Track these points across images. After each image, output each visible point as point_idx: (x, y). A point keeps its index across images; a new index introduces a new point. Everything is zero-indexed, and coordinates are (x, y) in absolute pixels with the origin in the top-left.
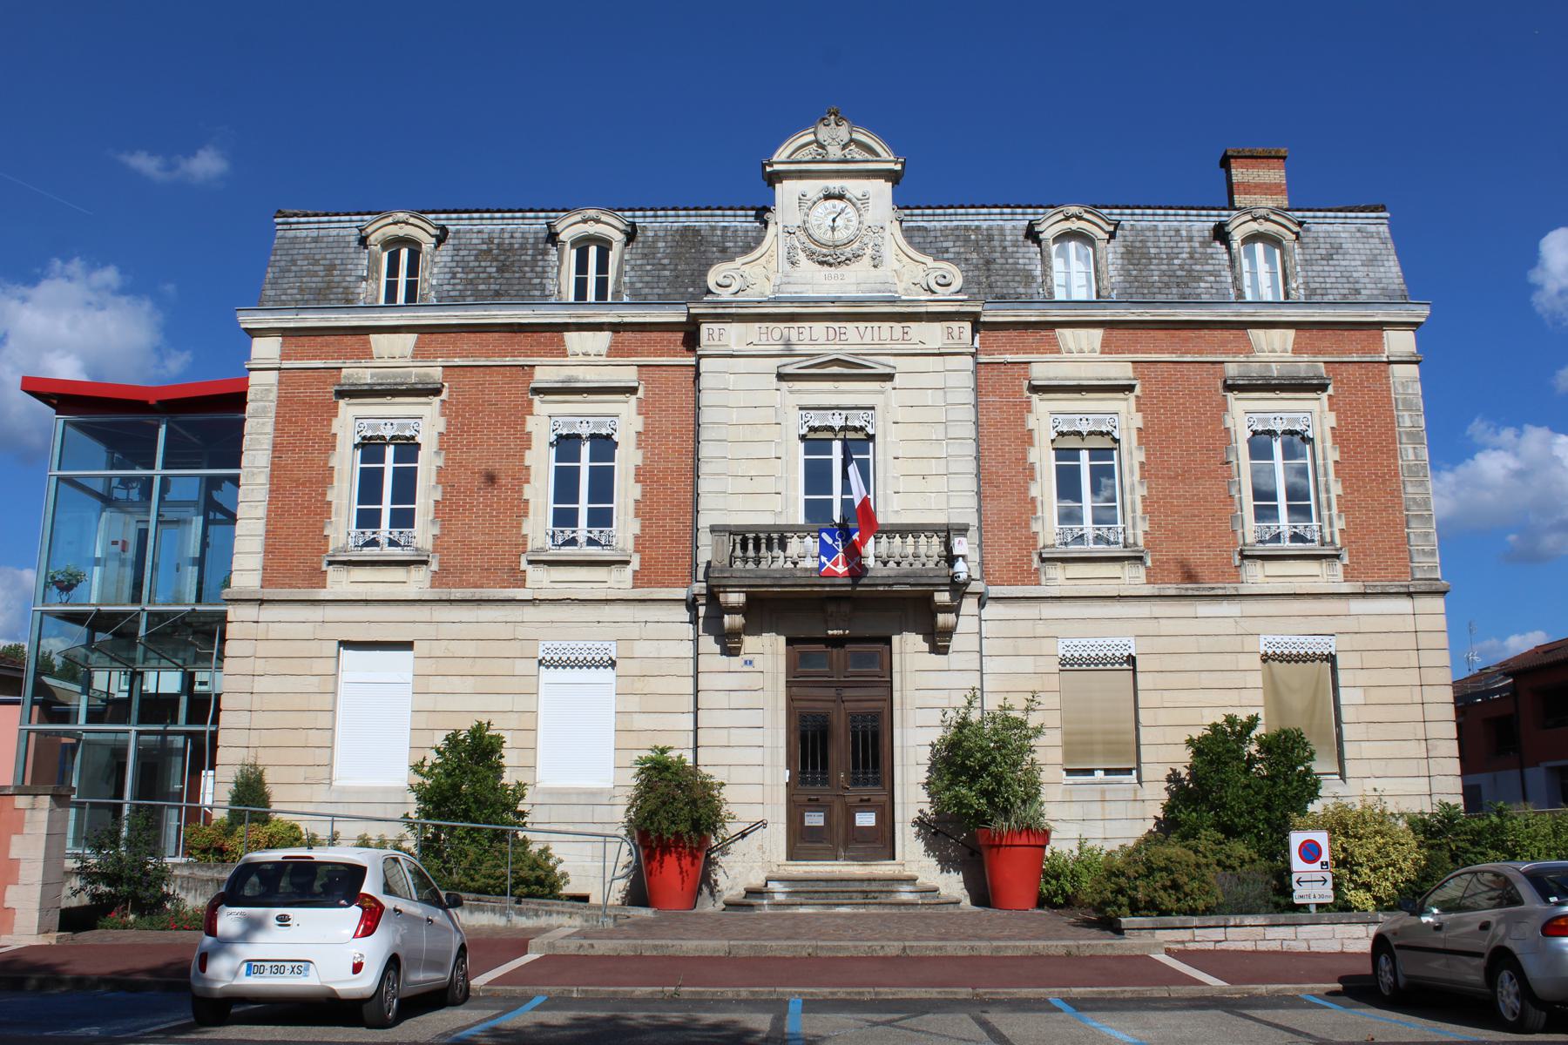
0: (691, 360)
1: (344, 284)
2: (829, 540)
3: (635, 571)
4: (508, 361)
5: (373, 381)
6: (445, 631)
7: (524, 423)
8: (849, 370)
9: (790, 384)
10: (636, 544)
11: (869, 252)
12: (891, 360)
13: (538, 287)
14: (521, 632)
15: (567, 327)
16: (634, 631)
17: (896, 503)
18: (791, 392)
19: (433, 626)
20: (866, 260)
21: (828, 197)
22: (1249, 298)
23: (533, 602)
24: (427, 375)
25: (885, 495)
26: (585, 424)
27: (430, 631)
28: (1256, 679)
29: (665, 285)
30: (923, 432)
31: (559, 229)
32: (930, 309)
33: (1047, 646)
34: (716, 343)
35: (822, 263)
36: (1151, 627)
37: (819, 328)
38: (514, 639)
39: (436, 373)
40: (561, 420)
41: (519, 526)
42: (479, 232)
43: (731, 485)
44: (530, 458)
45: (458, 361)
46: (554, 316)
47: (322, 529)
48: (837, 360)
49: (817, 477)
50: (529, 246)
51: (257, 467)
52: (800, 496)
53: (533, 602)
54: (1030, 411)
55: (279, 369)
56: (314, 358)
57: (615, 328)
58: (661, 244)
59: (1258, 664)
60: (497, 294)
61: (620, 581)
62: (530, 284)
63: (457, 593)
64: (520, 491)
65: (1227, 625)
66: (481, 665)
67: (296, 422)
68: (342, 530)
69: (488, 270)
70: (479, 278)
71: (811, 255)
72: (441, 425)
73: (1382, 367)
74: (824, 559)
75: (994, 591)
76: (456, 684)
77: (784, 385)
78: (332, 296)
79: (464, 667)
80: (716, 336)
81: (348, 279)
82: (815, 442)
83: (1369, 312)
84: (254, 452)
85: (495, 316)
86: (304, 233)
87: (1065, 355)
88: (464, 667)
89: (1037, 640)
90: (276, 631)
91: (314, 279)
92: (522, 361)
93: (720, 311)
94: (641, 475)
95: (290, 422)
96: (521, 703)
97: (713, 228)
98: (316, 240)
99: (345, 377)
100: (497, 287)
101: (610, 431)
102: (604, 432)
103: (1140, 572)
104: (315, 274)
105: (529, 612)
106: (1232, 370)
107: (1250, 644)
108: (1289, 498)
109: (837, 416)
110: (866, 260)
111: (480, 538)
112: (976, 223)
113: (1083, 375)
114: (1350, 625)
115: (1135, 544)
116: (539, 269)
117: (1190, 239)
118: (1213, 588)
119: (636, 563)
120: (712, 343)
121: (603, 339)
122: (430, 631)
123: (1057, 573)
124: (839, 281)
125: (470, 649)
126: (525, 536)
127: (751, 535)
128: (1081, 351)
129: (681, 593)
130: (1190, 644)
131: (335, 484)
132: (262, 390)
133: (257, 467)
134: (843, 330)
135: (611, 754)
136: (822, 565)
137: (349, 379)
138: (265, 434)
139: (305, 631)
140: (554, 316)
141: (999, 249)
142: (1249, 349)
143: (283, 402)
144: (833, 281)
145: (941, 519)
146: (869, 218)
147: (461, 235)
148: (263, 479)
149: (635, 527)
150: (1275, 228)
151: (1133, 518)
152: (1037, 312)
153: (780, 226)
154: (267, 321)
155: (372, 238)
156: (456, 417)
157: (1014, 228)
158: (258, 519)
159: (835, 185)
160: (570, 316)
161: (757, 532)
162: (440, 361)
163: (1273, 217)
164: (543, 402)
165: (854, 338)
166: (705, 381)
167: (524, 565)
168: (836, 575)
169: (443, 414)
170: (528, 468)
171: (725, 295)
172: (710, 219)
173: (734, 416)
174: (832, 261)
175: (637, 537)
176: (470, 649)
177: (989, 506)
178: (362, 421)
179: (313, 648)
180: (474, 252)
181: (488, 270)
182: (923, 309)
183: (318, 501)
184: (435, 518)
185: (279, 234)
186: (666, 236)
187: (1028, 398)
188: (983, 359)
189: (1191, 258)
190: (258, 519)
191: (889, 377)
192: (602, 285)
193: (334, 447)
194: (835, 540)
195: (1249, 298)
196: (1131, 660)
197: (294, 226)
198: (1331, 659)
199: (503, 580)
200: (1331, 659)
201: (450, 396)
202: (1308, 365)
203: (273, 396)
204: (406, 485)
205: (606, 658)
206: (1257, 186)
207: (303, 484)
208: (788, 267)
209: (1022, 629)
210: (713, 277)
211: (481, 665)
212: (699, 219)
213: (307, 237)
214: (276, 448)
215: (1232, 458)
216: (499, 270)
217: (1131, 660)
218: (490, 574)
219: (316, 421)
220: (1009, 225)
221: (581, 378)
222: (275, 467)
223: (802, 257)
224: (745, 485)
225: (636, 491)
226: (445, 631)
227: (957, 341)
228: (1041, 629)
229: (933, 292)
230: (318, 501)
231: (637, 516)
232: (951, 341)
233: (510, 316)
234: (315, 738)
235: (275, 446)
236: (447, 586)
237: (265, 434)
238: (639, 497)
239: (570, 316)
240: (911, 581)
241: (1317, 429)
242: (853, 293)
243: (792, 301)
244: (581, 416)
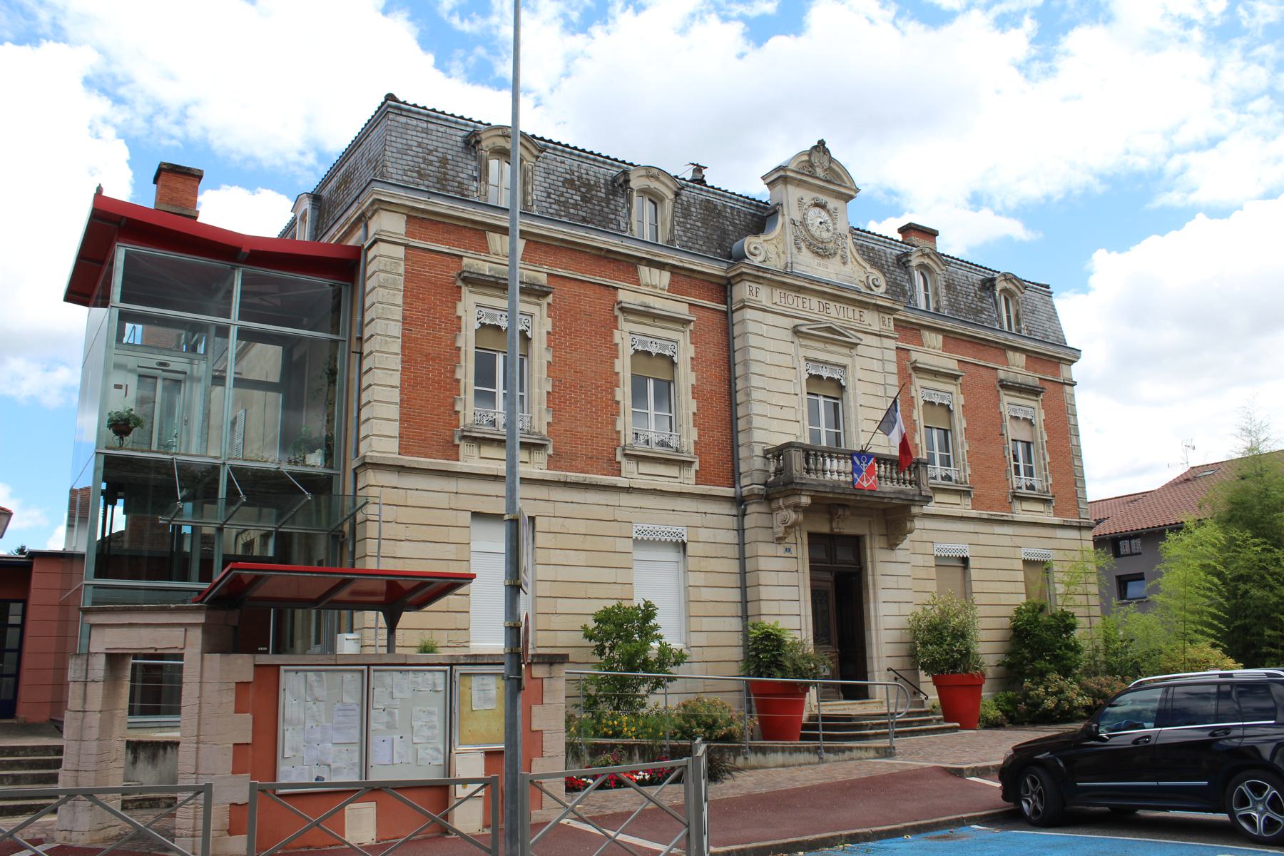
0: (723, 307)
1: (458, 179)
2: (858, 463)
3: (696, 471)
4: (598, 280)
5: (490, 274)
6: (562, 509)
7: (612, 335)
8: (833, 336)
9: (801, 340)
10: (696, 449)
11: (840, 252)
12: (859, 335)
13: (614, 222)
14: (620, 514)
15: (641, 260)
16: (697, 520)
18: (801, 346)
19: (551, 504)
20: (838, 257)
21: (817, 205)
22: (1024, 333)
23: (629, 490)
24: (536, 278)
25: (857, 432)
26: (654, 344)
28: (1021, 576)
29: (701, 243)
31: (632, 177)
32: (879, 302)
33: (928, 548)
34: (754, 298)
35: (817, 254)
36: (974, 539)
37: (815, 302)
38: (614, 521)
39: (543, 279)
40: (638, 337)
41: (614, 423)
42: (562, 162)
45: (561, 272)
46: (636, 250)
47: (453, 405)
48: (830, 327)
50: (602, 185)
51: (390, 337)
53: (629, 490)
54: (911, 384)
55: (406, 246)
56: (437, 241)
57: (674, 269)
58: (693, 209)
59: (1020, 565)
60: (584, 220)
61: (686, 480)
62: (607, 217)
63: (573, 476)
64: (613, 394)
65: (1006, 541)
66: (590, 543)
67: (423, 299)
69: (575, 197)
70: (568, 202)
71: (808, 247)
72: (548, 325)
73: (1061, 386)
74: (855, 475)
76: (573, 558)
77: (796, 340)
78: (449, 188)
79: (577, 542)
80: (754, 292)
81: (460, 175)
83: (1058, 351)
84: (387, 322)
85: (592, 240)
86: (414, 122)
87: (926, 348)
88: (577, 542)
89: (923, 544)
90: (413, 498)
91: (430, 168)
93: (760, 274)
94: (696, 392)
95: (418, 298)
96: (621, 576)
97: (725, 206)
99: (466, 265)
100: (584, 214)
101: (671, 354)
102: (667, 353)
103: (968, 501)
104: (430, 163)
105: (625, 499)
106: (1002, 375)
109: (824, 369)
110: (838, 257)
111: (584, 429)
112: (872, 245)
113: (936, 364)
114: (1056, 544)
115: (966, 482)
116: (612, 207)
118: (1003, 516)
119: (696, 466)
120: (751, 297)
121: (664, 278)
122: (548, 508)
123: (939, 497)
124: (825, 269)
125: (581, 527)
126: (619, 432)
127: (812, 453)
128: (934, 348)
129: (729, 492)
131: (463, 363)
133: (390, 337)
134: (828, 306)
135: (472, 610)
136: (854, 480)
137: (470, 268)
138: (396, 305)
139: (442, 500)
140: (636, 250)
141: (886, 267)
142: (1006, 363)
144: (821, 268)
147: (549, 161)
149: (694, 435)
150: (1013, 288)
151: (964, 465)
152: (916, 317)
153: (787, 219)
154: (400, 197)
155: (484, 144)
156: (560, 320)
157: (891, 254)
158: (392, 387)
159: (823, 198)
160: (647, 253)
161: (816, 451)
162: (546, 269)
163: (1014, 281)
164: (625, 320)
165: (837, 314)
167: (619, 458)
168: (863, 489)
169: (549, 316)
170: (617, 374)
172: (722, 198)
173: (768, 358)
174: (822, 253)
175: (695, 443)
176: (581, 527)
178: (481, 309)
179: (449, 517)
180: (562, 179)
181: (575, 197)
182: (874, 301)
183: (447, 377)
184: (548, 407)
185: (391, 116)
186: (695, 203)
187: (910, 374)
189: (976, 297)
190: (392, 387)
191: (853, 346)
193: (459, 329)
194: (861, 463)
195: (1024, 333)
196: (965, 561)
197: (404, 113)
199: (603, 469)
201: (554, 300)
202: (1031, 379)
203: (401, 270)
205: (680, 541)
207: (433, 359)
208: (795, 251)
211: (590, 543)
212: (714, 196)
213: (417, 126)
214: (405, 320)
215: (1005, 432)
216: (584, 199)
217: (965, 561)
218: (592, 462)
219: (441, 301)
220: (889, 251)
221: (652, 305)
222: (407, 340)
223: (803, 245)
225: (693, 406)
226: (562, 509)
227: (887, 328)
229: (872, 290)
230: (447, 377)
231: (694, 426)
232: (884, 327)
233: (604, 242)
235: (404, 318)
236: (559, 468)
237: (396, 305)
238: (696, 411)
239: (647, 253)
240: (903, 497)
241: (1037, 419)
242: (833, 279)
243: (805, 278)
244: (658, 338)
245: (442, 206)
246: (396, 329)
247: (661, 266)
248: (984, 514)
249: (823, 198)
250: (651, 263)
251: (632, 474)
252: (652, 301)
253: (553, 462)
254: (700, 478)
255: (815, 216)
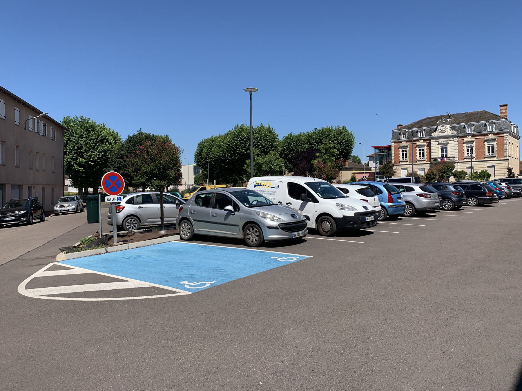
14: (417, 166)
17: (449, 154)
27: (409, 167)
30: (452, 147)
43: (434, 153)
44: (417, 151)
45: (410, 143)
49: (442, 152)
52: (441, 154)
68: (401, 159)
71: (441, 132)
75: (459, 161)
82: (442, 149)
92: (415, 143)
98: (396, 132)
107: (486, 165)
108: (492, 150)
117: (482, 125)
119: (426, 160)
121: (422, 141)
122: (409, 167)
130: (479, 165)
132: (393, 147)
143: (394, 148)
145: (453, 156)
146: (446, 128)
148: (394, 154)
162: (408, 143)
166: (432, 144)
171: (433, 136)
177: (459, 153)
188: (459, 139)
192: (422, 135)
198: (494, 167)
200: (494, 167)
204: (406, 154)
206: (503, 109)
209: (462, 164)
210: (432, 134)
224: (435, 153)
228: (464, 164)
234: (400, 176)
245: (397, 141)
246: (393, 153)
247: (422, 140)
248: (477, 160)
249: (443, 125)
250: (420, 140)
251: (418, 162)
252: (421, 144)
253: (409, 162)
254: (427, 162)
255: (442, 128)
